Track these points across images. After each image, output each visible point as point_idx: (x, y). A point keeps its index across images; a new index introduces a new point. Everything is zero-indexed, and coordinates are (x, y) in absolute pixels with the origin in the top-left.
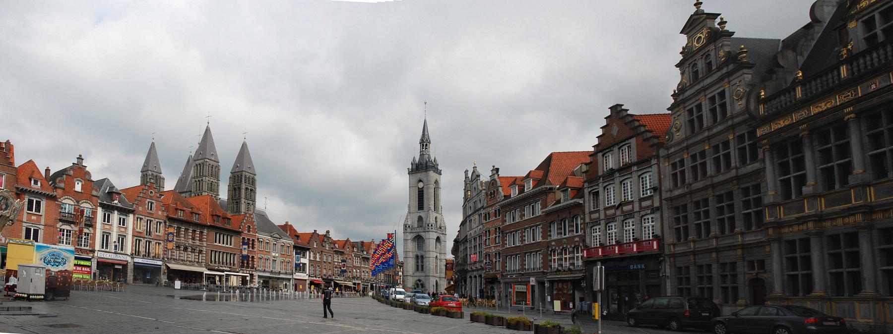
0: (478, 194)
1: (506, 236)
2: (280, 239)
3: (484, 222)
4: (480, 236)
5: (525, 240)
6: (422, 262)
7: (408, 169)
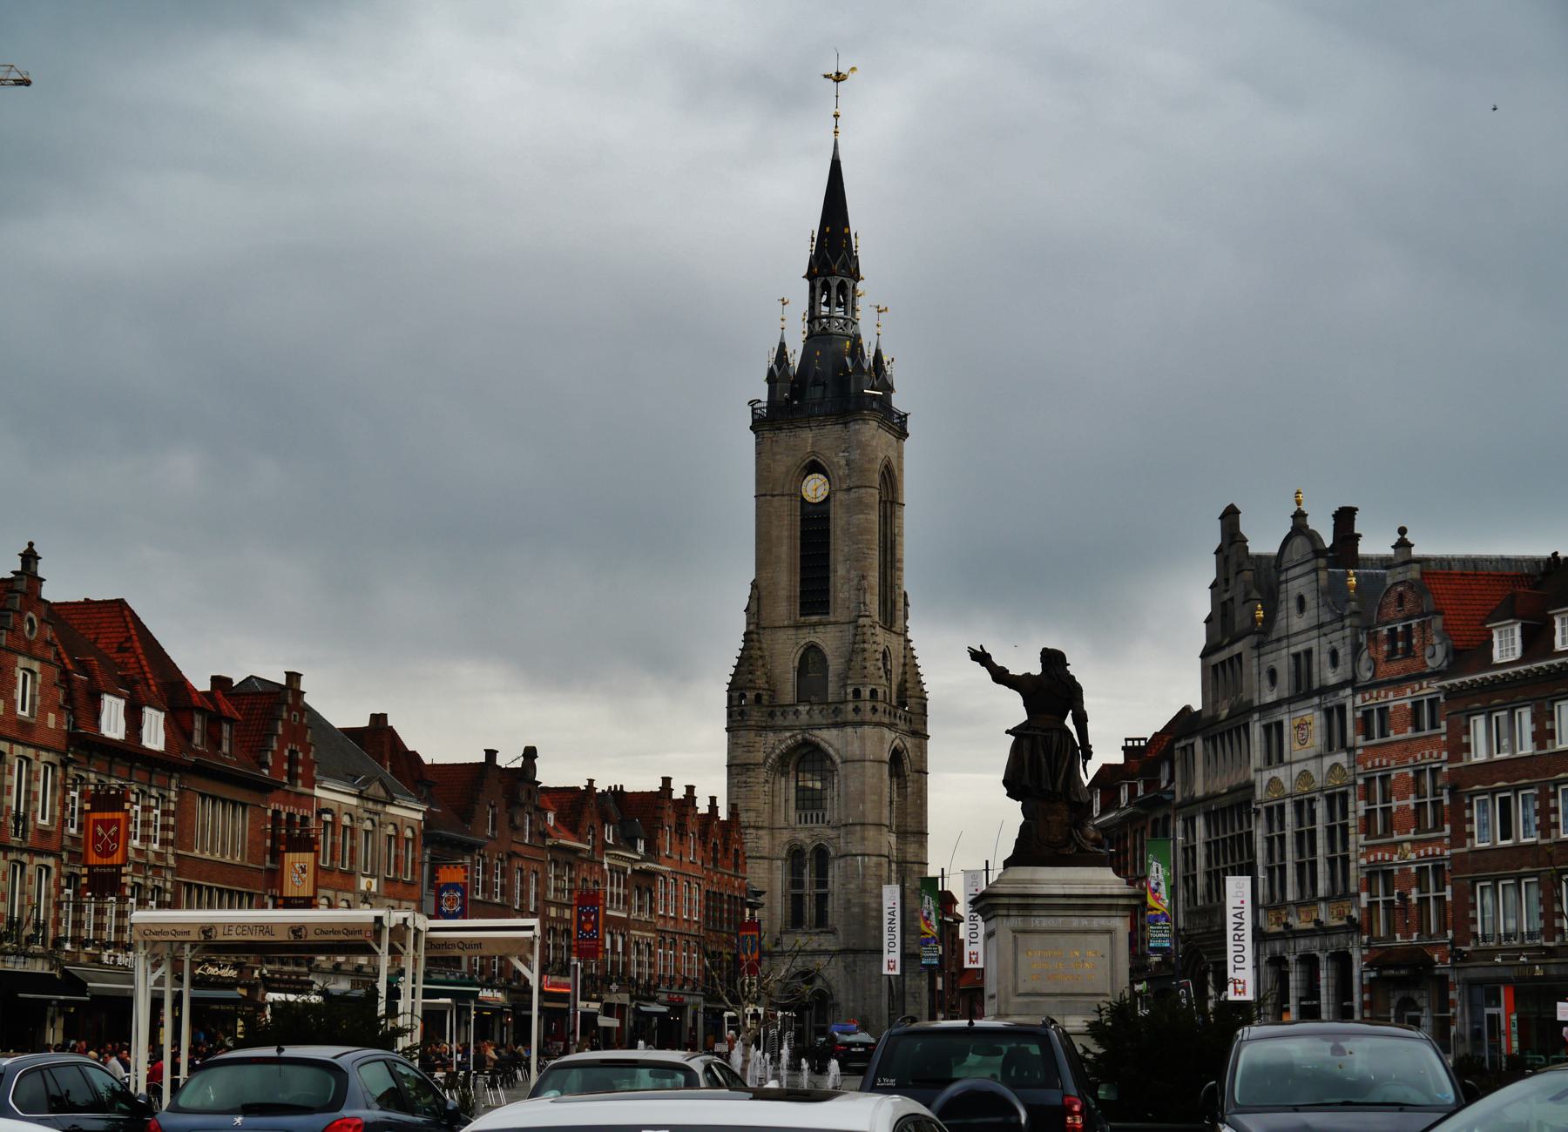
0: (1320, 626)
1: (1471, 806)
2: (385, 804)
3: (1360, 741)
4: (1336, 801)
5: (1556, 825)
6: (822, 883)
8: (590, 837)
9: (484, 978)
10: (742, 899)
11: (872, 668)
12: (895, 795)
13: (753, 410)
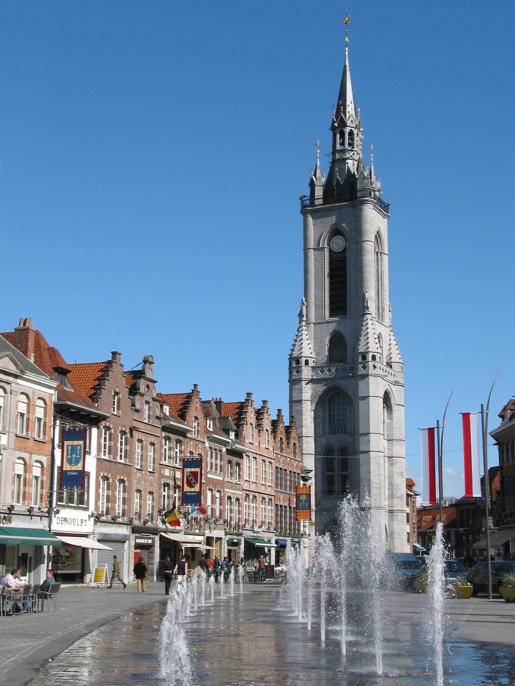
2: (16, 376)
7: (302, 198)
8: (196, 424)
9: (109, 517)
10: (298, 474)
11: (372, 343)
12: (386, 418)
13: (302, 202)
